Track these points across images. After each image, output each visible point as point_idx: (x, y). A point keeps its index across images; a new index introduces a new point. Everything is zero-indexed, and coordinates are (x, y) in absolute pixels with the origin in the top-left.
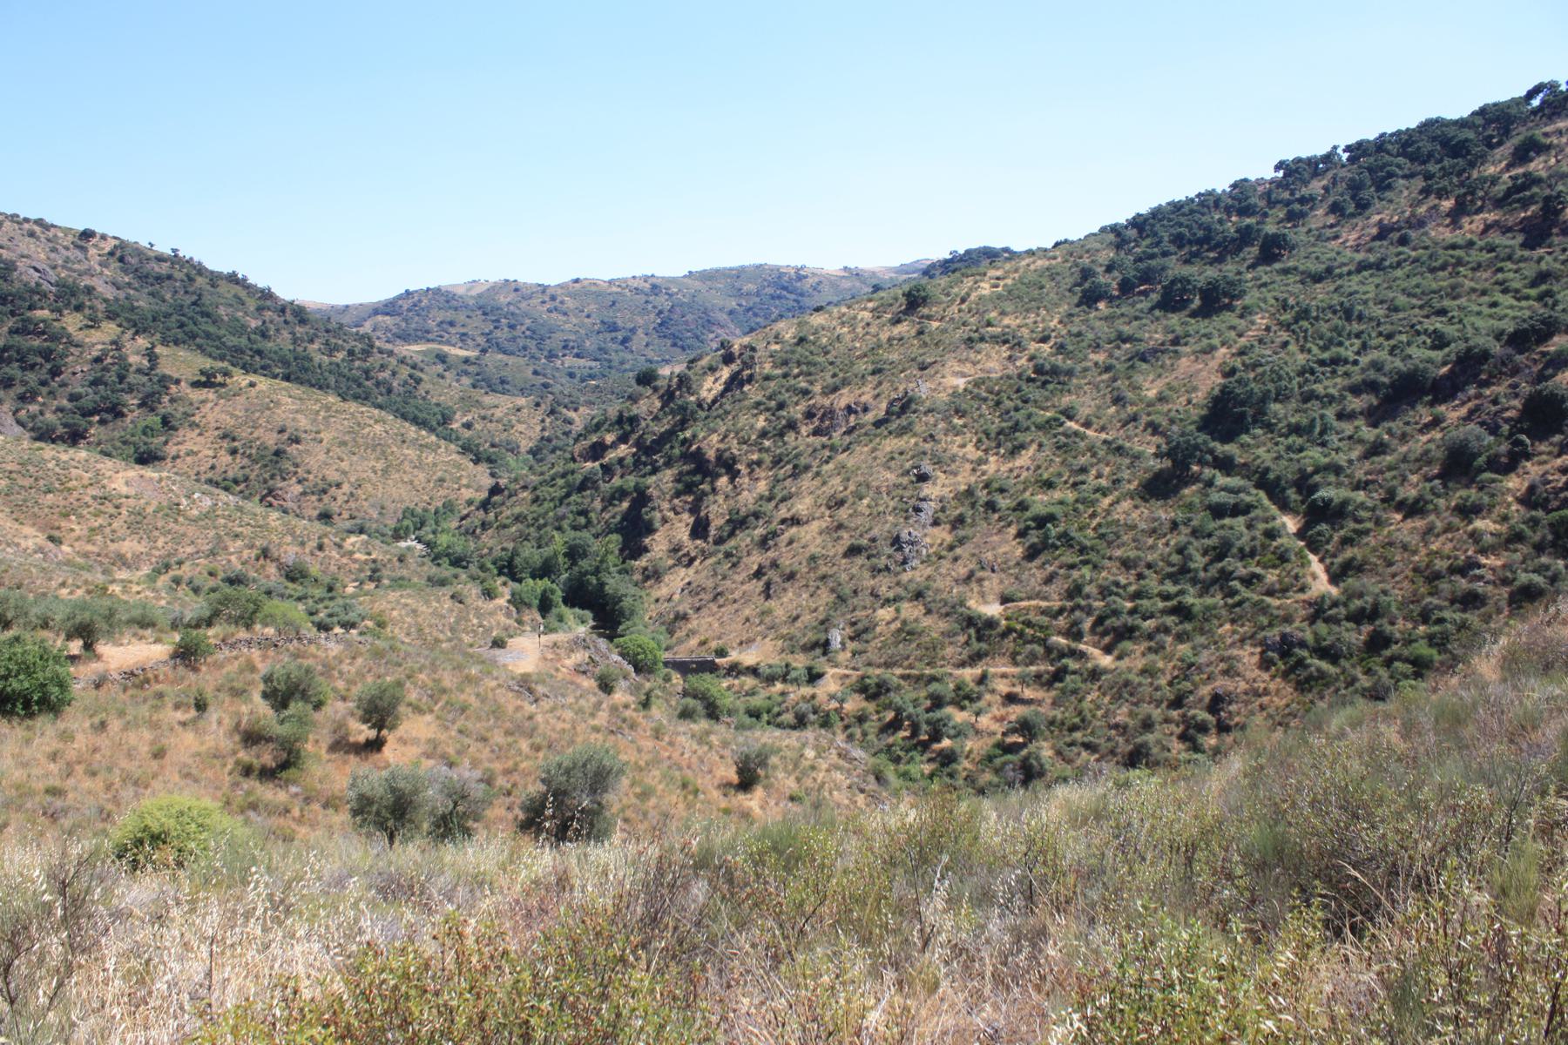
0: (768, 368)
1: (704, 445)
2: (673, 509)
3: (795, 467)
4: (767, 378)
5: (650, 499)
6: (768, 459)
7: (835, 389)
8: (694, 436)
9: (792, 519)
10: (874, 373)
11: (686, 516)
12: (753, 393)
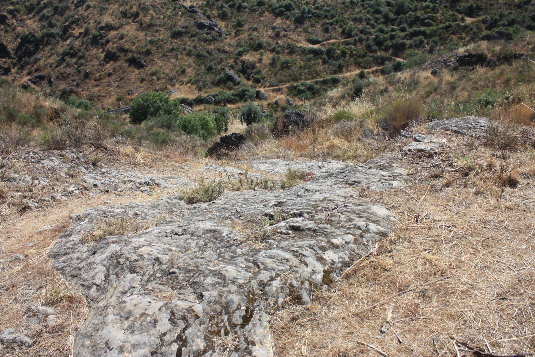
3: (56, 9)
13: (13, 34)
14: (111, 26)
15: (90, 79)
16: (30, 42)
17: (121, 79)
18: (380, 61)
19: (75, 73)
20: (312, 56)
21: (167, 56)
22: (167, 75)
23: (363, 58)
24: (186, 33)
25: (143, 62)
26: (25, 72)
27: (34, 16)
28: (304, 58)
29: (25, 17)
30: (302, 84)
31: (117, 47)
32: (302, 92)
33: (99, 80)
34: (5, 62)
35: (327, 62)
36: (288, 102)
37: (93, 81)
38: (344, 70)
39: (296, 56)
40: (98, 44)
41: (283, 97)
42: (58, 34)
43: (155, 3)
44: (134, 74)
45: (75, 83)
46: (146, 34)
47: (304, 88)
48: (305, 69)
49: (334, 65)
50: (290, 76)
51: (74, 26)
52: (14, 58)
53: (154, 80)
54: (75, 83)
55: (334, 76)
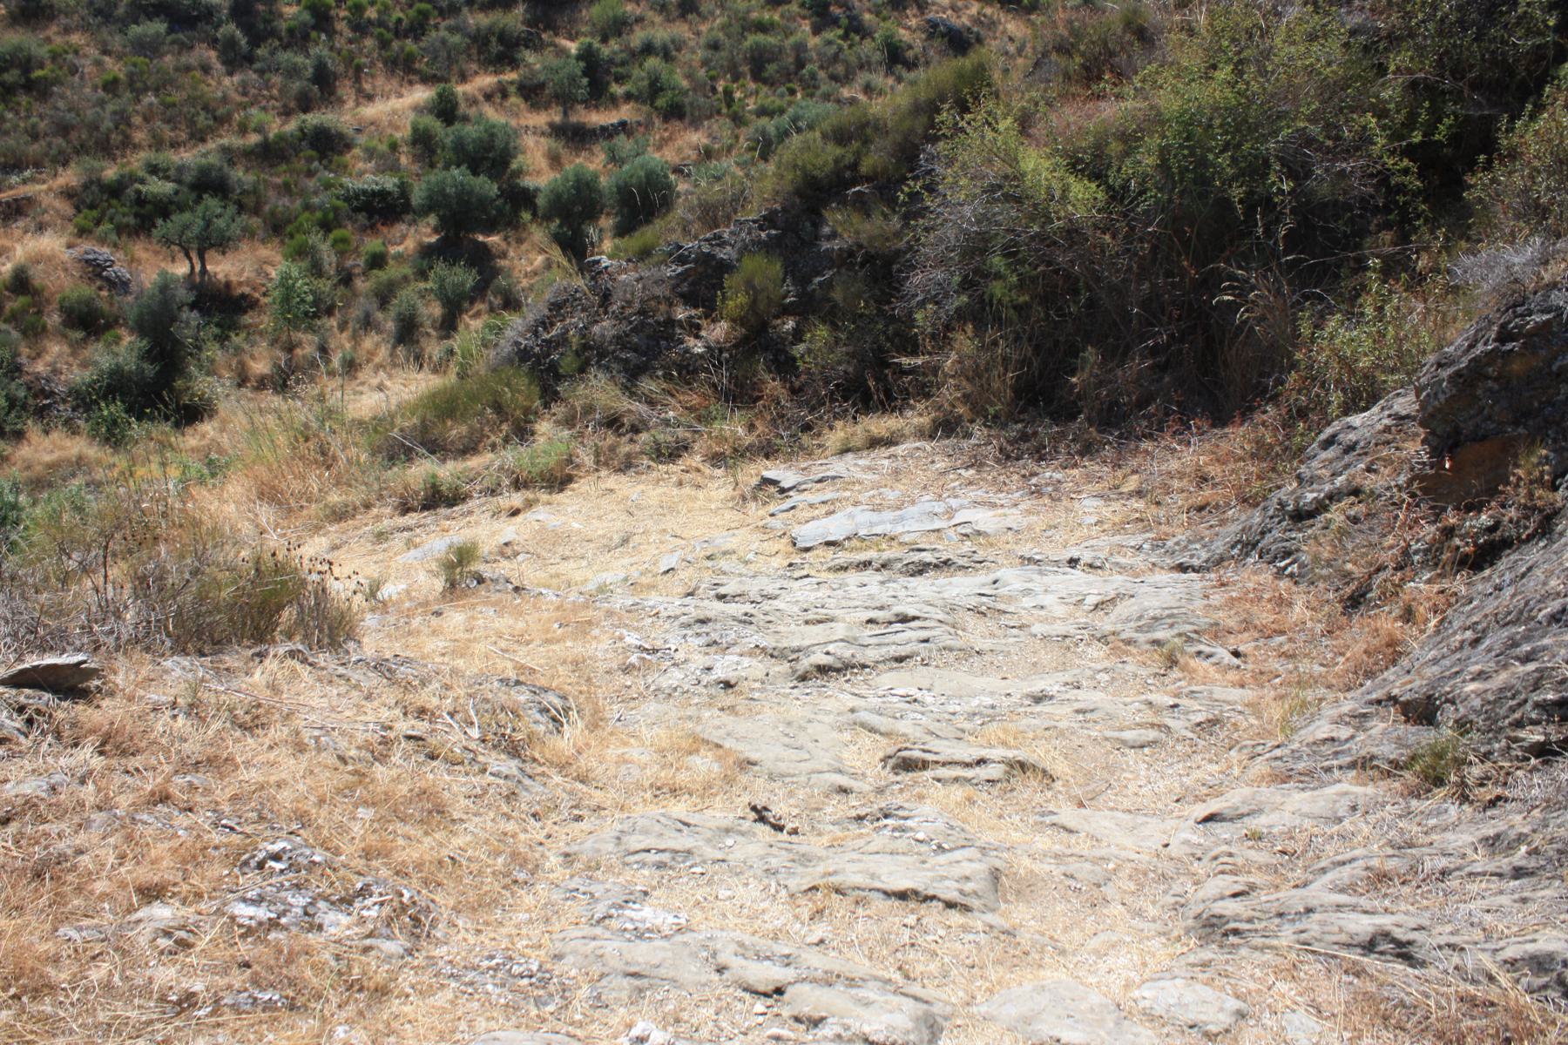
18: (495, 47)
20: (158, 27)
23: (417, 39)
28: (117, 42)
30: (154, 169)
32: (164, 208)
35: (249, 59)
36: (95, 270)
38: (345, 90)
39: (67, 30)
41: (51, 243)
47: (169, 187)
48: (138, 93)
49: (293, 72)
50: (64, 129)
55: (313, 119)
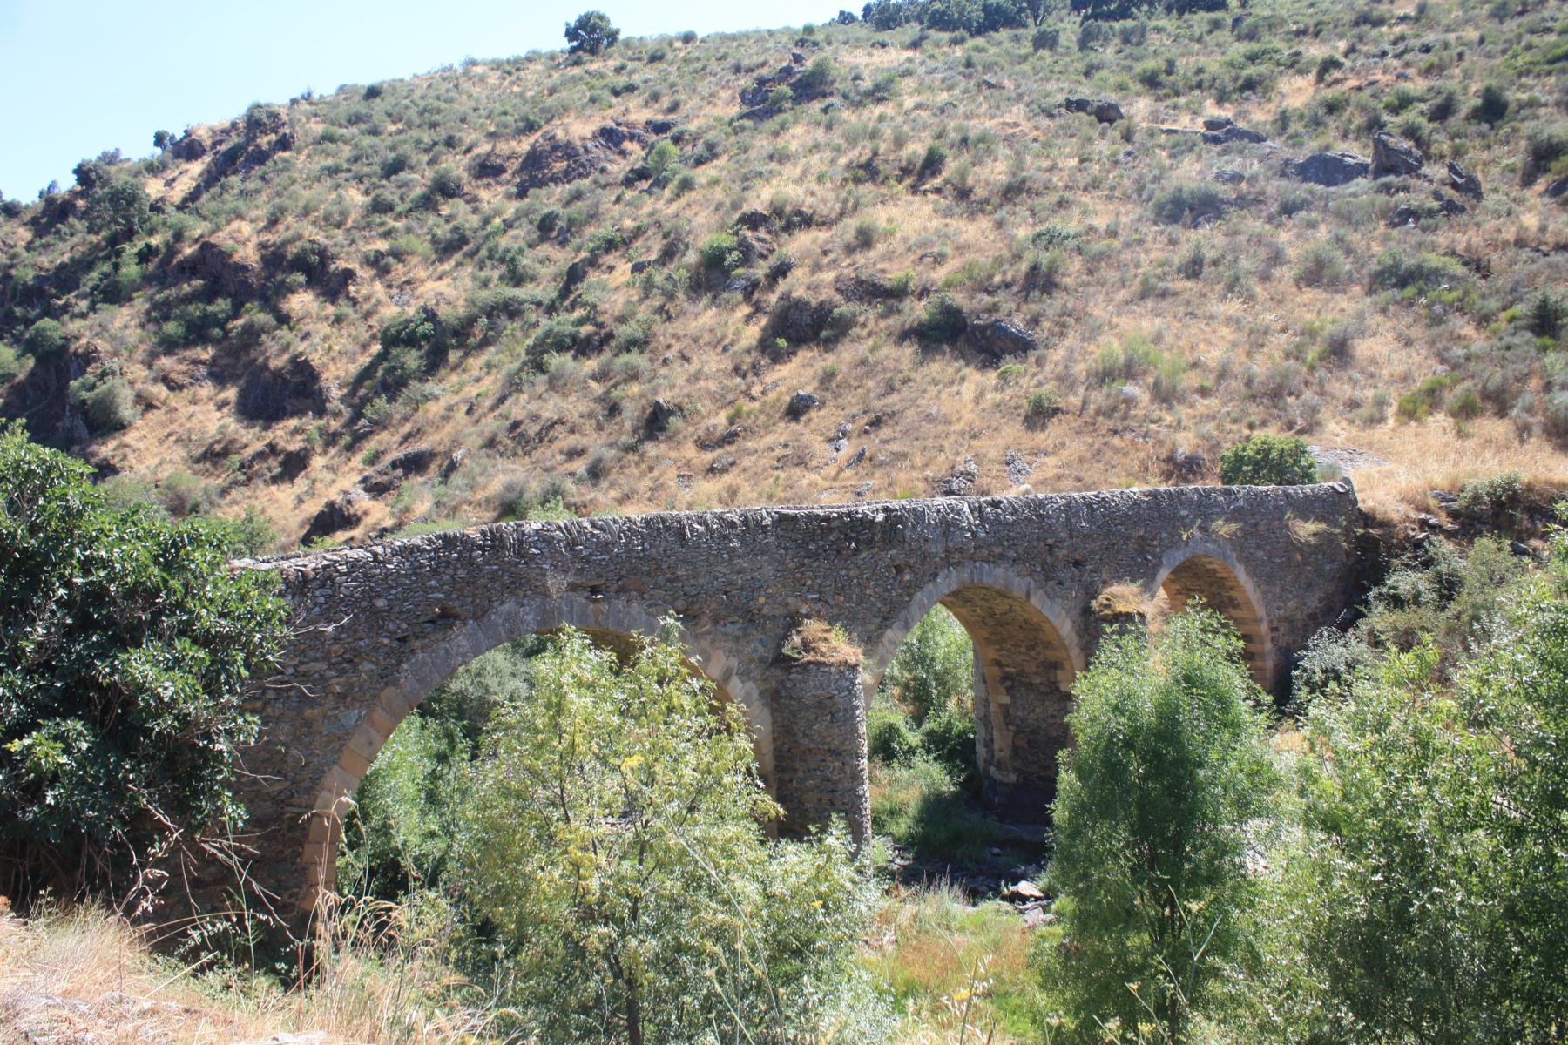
0: (318, 128)
1: (222, 239)
2: (165, 380)
4: (328, 138)
5: (88, 357)
6: (424, 247)
7: (530, 127)
8: (179, 236)
9: (778, 211)
10: (616, 93)
11: (206, 390)
12: (302, 161)
13: (363, 328)
14: (799, 213)
15: (674, 440)
16: (411, 341)
17: (876, 423)
19: (590, 415)
21: (1164, 294)
22: (1223, 374)
24: (1242, 202)
25: (1018, 324)
26: (357, 460)
27: (459, 264)
29: (422, 274)
31: (837, 280)
33: (729, 438)
34: (296, 431)
37: (690, 451)
40: (727, 288)
42: (539, 304)
43: (1011, 131)
44: (962, 391)
45: (580, 466)
46: (999, 225)
51: (608, 259)
52: (337, 414)
53: (1130, 401)
54: (580, 466)
